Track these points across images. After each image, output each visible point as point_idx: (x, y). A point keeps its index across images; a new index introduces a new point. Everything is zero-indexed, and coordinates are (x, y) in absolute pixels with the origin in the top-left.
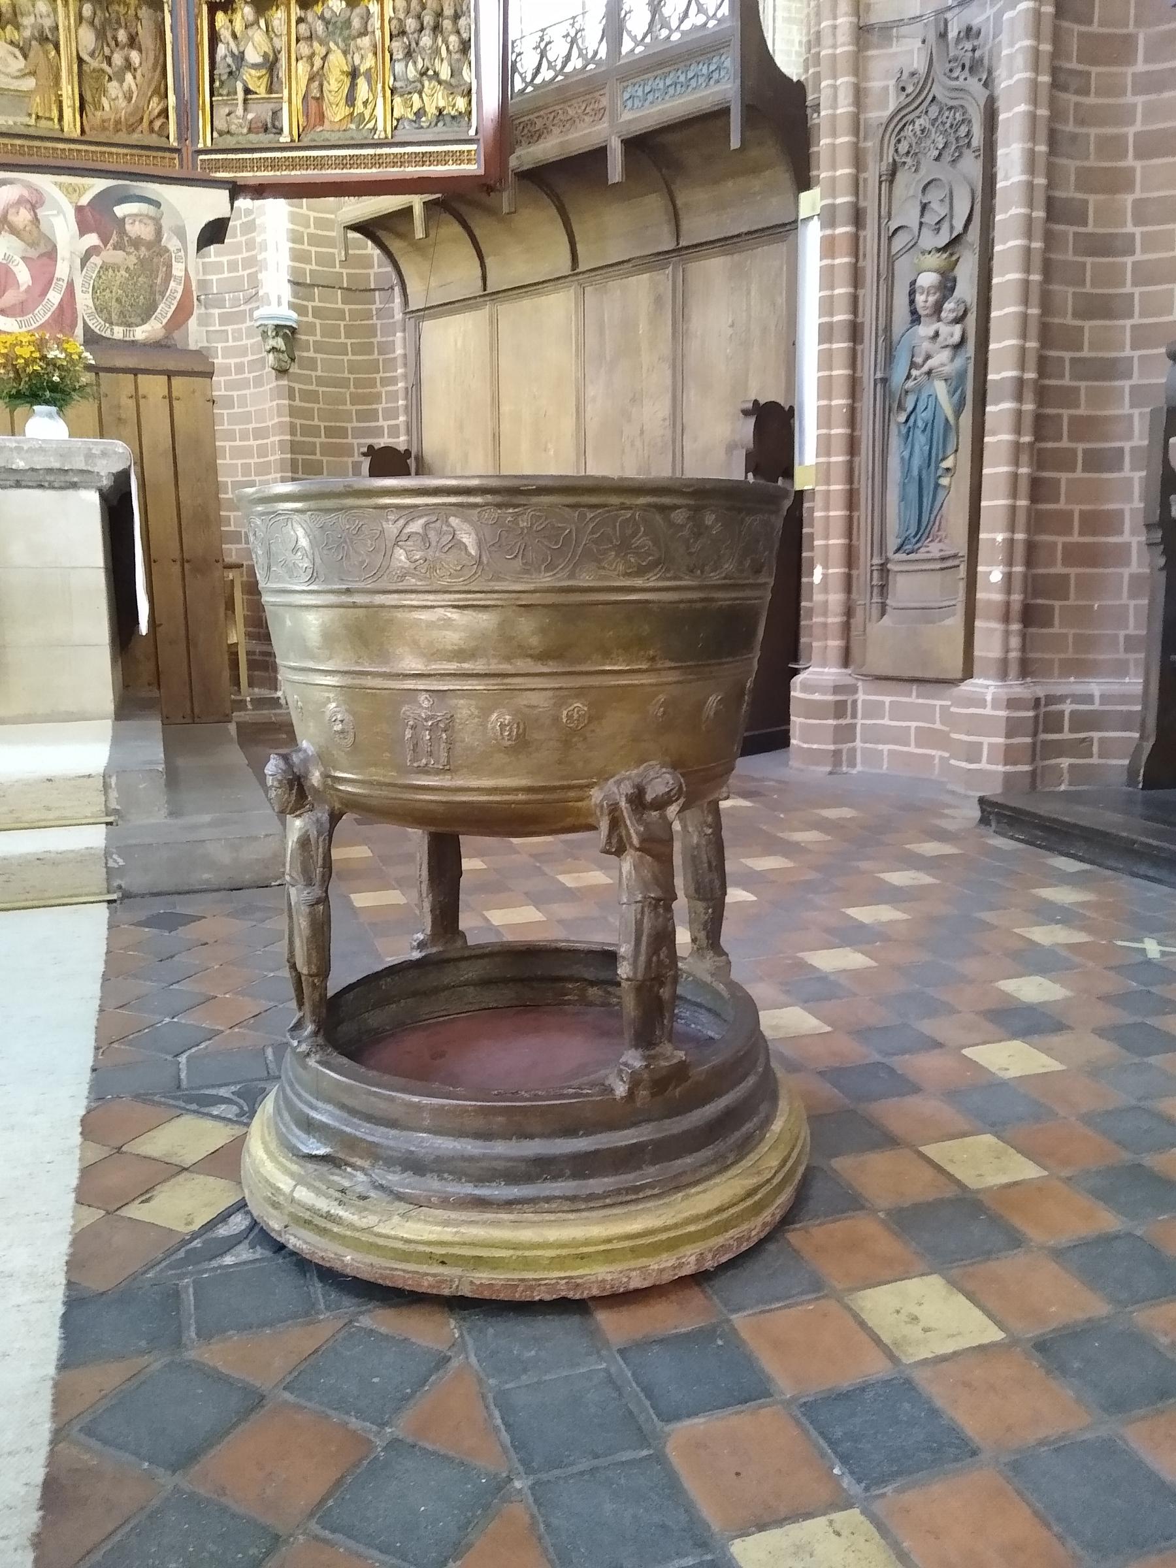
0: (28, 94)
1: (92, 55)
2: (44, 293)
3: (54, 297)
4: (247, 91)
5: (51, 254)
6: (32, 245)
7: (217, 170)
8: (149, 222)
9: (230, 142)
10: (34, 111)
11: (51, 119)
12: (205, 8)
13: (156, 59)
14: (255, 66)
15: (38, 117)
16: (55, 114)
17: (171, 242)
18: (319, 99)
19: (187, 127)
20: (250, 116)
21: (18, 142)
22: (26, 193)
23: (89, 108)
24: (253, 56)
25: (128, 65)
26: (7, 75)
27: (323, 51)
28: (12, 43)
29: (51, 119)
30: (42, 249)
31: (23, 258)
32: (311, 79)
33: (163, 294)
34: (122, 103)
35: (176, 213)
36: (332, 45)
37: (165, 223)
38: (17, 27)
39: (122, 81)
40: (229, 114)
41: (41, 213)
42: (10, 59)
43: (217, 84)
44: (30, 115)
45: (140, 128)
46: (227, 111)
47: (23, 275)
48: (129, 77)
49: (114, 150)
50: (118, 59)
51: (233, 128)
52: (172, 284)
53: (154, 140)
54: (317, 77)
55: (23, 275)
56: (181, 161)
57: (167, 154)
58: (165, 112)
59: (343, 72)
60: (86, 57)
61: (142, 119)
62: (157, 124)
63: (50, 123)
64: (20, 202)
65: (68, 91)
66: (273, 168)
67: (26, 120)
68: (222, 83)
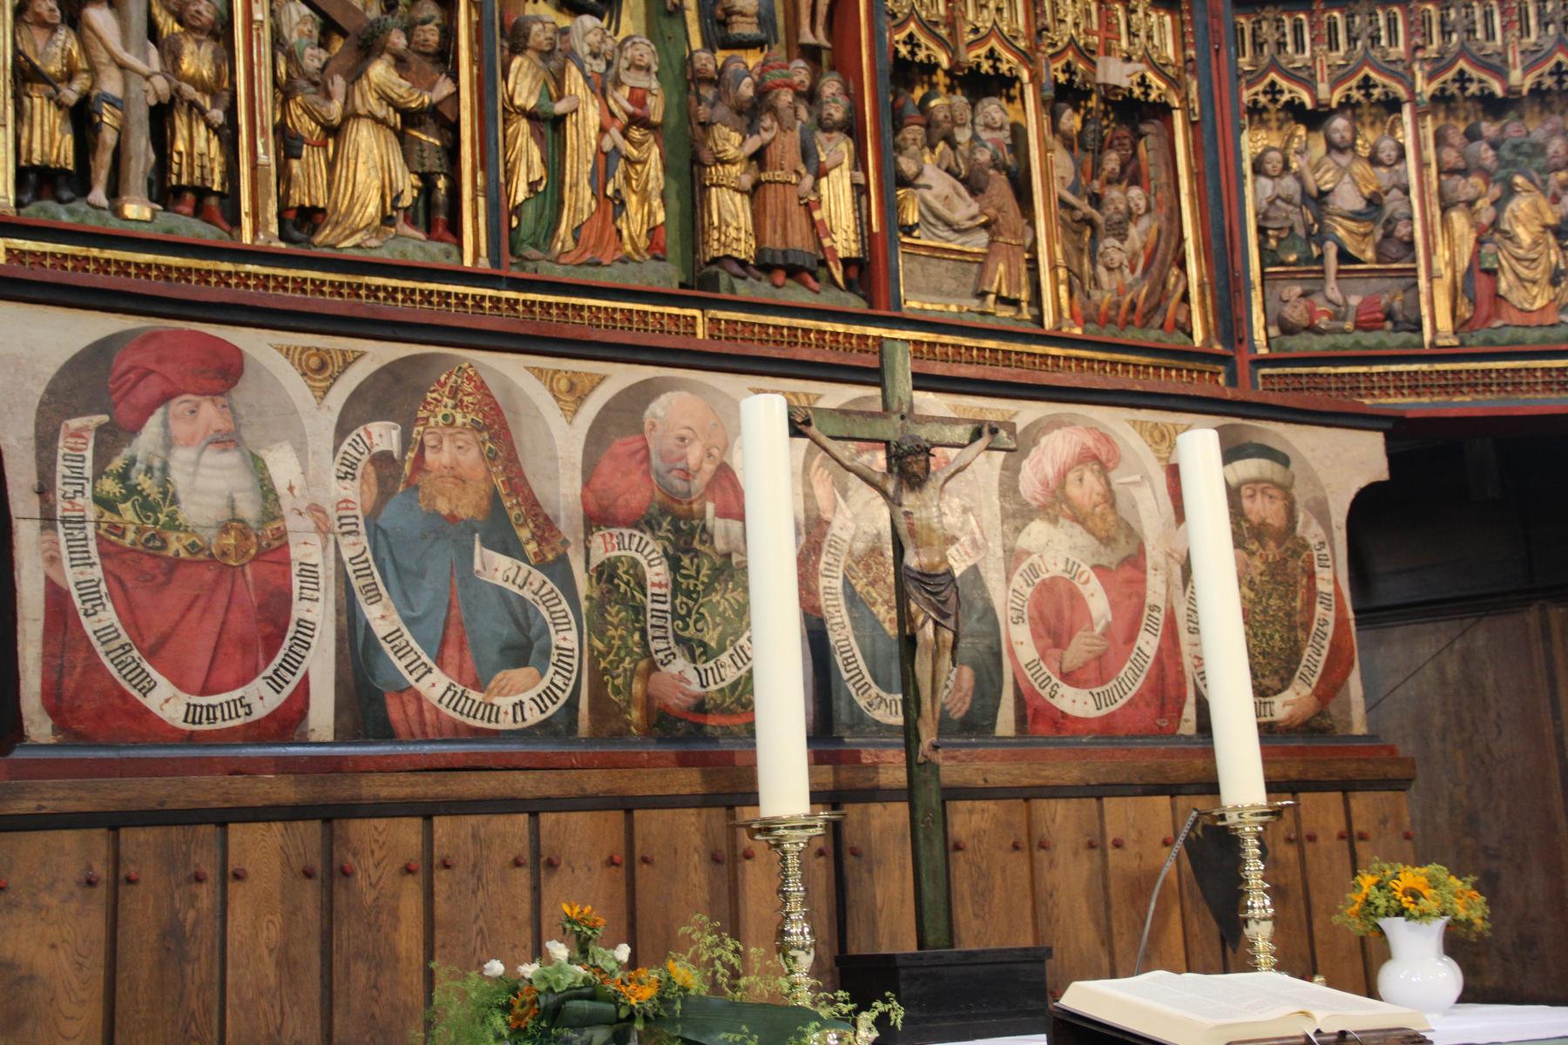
0: (982, 262)
2: (1131, 638)
3: (1148, 643)
4: (1344, 256)
5: (1136, 561)
6: (1107, 541)
8: (1274, 492)
9: (1317, 345)
10: (994, 289)
11: (1015, 303)
14: (1355, 216)
16: (1024, 295)
17: (1310, 531)
18: (1492, 273)
19: (1230, 322)
20: (1354, 301)
22: (1090, 443)
24: (1348, 198)
26: (949, 225)
27: (1495, 191)
30: (1124, 549)
31: (1095, 568)
32: (1480, 242)
33: (1307, 627)
35: (1312, 479)
36: (1519, 180)
37: (1300, 493)
39: (1123, 237)
40: (1304, 295)
41: (1117, 478)
43: (1273, 242)
44: (982, 295)
45: (1157, 320)
46: (1298, 290)
47: (1098, 604)
48: (1133, 231)
49: (1133, 358)
51: (1323, 322)
52: (1319, 609)
54: (1491, 232)
55: (1098, 604)
57: (1209, 367)
59: (1546, 227)
64: (1087, 457)
66: (1414, 390)
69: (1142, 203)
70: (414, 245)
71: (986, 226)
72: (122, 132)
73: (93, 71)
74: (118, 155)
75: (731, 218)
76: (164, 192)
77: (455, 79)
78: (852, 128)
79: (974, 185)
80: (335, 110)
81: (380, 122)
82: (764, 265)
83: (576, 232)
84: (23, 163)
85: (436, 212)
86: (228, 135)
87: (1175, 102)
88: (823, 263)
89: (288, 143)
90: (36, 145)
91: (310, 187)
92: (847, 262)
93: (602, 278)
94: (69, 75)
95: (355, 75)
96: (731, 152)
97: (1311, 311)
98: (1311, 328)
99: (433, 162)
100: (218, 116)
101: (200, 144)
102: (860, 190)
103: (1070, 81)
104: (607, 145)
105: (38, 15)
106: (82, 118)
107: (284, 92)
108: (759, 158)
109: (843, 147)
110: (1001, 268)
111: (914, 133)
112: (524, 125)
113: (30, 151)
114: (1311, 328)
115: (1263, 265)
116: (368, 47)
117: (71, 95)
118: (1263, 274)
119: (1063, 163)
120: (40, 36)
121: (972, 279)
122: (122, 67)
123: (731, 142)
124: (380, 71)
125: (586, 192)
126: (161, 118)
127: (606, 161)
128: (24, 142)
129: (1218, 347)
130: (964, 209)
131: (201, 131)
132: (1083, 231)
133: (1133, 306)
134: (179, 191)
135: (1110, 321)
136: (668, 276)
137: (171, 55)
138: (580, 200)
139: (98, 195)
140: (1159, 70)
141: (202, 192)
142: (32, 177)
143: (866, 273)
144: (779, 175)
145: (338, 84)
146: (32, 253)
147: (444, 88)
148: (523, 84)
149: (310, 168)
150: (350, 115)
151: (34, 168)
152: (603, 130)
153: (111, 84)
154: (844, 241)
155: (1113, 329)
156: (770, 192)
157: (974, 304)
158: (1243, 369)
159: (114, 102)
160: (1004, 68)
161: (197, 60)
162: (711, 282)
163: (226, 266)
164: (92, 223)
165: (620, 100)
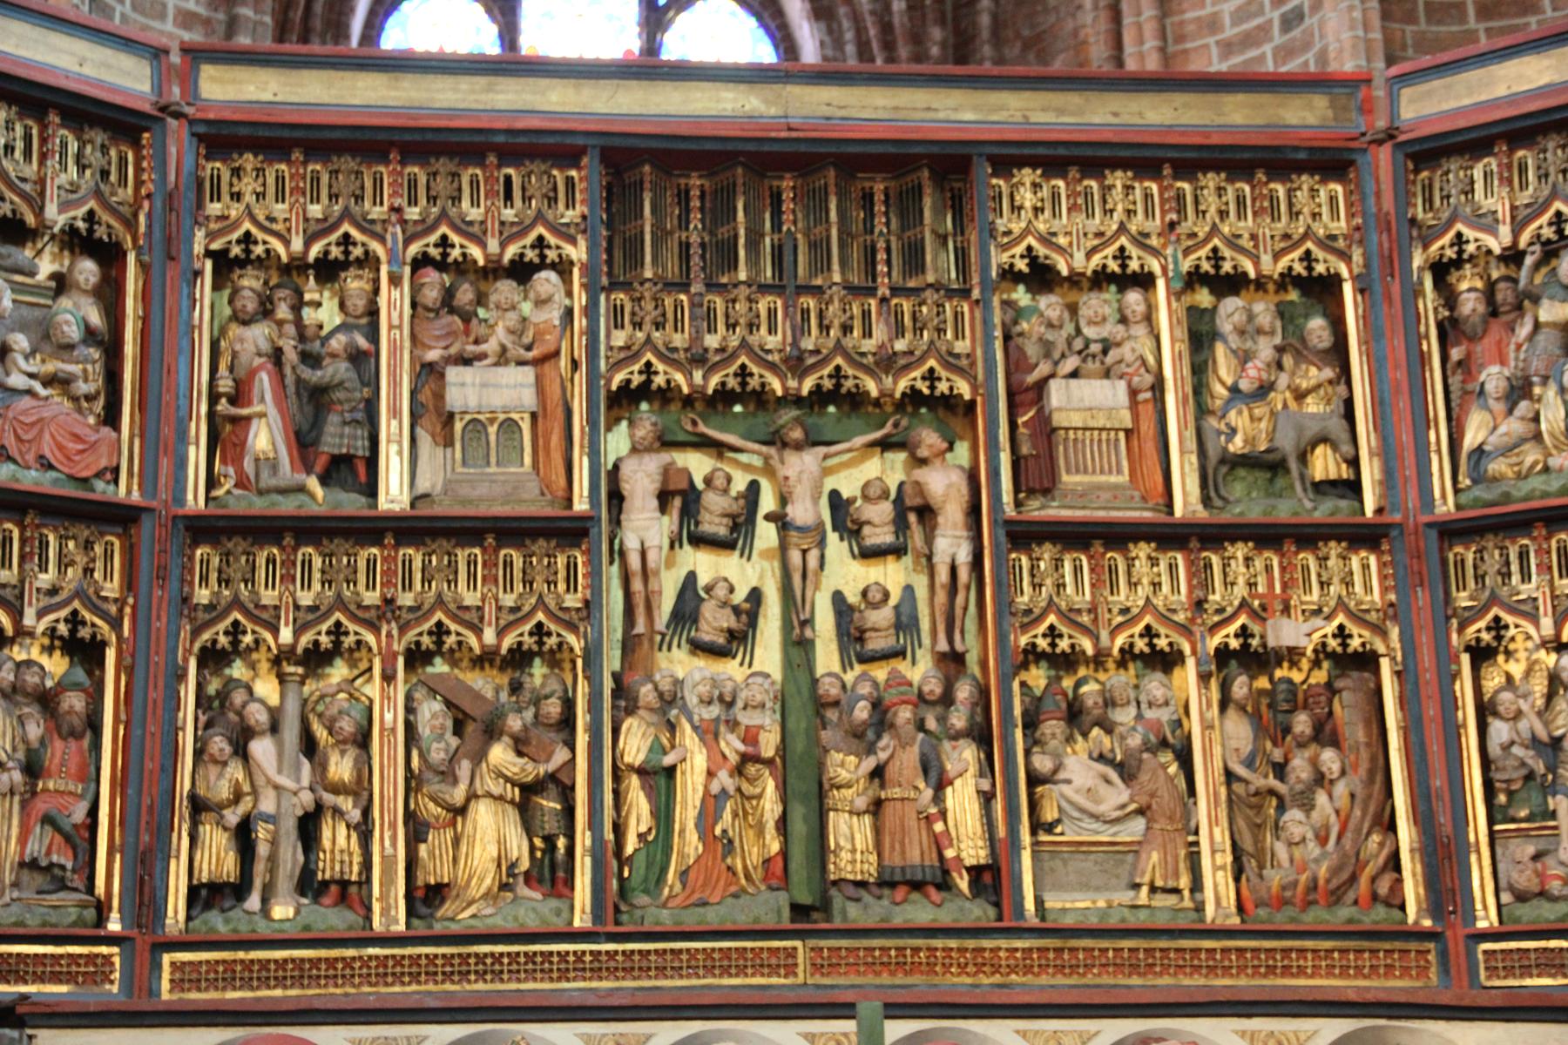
0: (1135, 849)
1: (1249, 763)
7: (1526, 971)
9: (1547, 913)
10: (1146, 879)
11: (1176, 891)
12: (1465, 659)
13: (1373, 759)
15: (1153, 889)
16: (1184, 882)
21: (1126, 944)
23: (1251, 865)
25: (1320, 779)
26: (1096, 817)
28: (1101, 758)
29: (1176, 891)
34: (1313, 849)
38: (1109, 729)
40: (1536, 857)
42: (1103, 789)
43: (1502, 798)
45: (1351, 896)
46: (1531, 849)
48: (1321, 798)
50: (1300, 766)
53: (1379, 916)
56: (1444, 956)
57: (1413, 945)
58: (1394, 862)
60: (1241, 770)
61: (1353, 878)
62: (1383, 888)
63: (1171, 900)
65: (1213, 837)
67: (1127, 897)
68: (1511, 794)
69: (1336, 767)
70: (532, 909)
71: (1141, 812)
72: (274, 843)
73: (255, 792)
74: (272, 859)
75: (852, 842)
76: (309, 884)
77: (572, 749)
78: (981, 736)
79: (1127, 771)
80: (458, 794)
81: (500, 798)
82: (887, 882)
83: (684, 875)
84: (195, 882)
85: (551, 872)
86: (364, 831)
87: (1381, 648)
88: (946, 872)
89: (416, 830)
90: (205, 866)
91: (435, 870)
92: (976, 872)
93: (712, 917)
94: (237, 797)
95: (479, 756)
96: (844, 775)
97: (1541, 876)
98: (1543, 894)
99: (551, 825)
100: (355, 815)
101: (341, 841)
102: (987, 798)
103: (1245, 646)
104: (715, 788)
105: (212, 755)
106: (243, 835)
107: (413, 783)
108: (878, 773)
109: (968, 753)
110: (1155, 857)
111: (1052, 728)
112: (635, 781)
113: (201, 871)
114: (1543, 894)
115: (1491, 822)
116: (492, 732)
117: (232, 817)
118: (1492, 835)
119: (1239, 731)
120: (213, 771)
121: (1124, 871)
122: (277, 787)
123: (846, 767)
124: (500, 754)
125: (692, 837)
126: (309, 827)
127: (712, 805)
128: (196, 864)
129: (1427, 923)
130: (1116, 796)
131: (342, 831)
132: (1253, 809)
133: (1313, 886)
134: (325, 884)
135: (1282, 902)
136: (770, 907)
137: (320, 767)
138: (689, 843)
139: (254, 902)
140: (1358, 618)
141: (344, 884)
142: (204, 892)
143: (991, 879)
144: (895, 792)
145: (464, 768)
146: (191, 963)
147: (561, 755)
148: (636, 743)
149: (435, 846)
150: (472, 796)
151: (203, 885)
152: (710, 774)
153: (267, 805)
154: (971, 849)
155: (1289, 911)
156: (889, 810)
157: (1127, 897)
158: (1456, 946)
159: (268, 819)
160: (1162, 643)
161: (341, 767)
162: (825, 906)
163: (350, 952)
164: (244, 929)
165: (732, 745)
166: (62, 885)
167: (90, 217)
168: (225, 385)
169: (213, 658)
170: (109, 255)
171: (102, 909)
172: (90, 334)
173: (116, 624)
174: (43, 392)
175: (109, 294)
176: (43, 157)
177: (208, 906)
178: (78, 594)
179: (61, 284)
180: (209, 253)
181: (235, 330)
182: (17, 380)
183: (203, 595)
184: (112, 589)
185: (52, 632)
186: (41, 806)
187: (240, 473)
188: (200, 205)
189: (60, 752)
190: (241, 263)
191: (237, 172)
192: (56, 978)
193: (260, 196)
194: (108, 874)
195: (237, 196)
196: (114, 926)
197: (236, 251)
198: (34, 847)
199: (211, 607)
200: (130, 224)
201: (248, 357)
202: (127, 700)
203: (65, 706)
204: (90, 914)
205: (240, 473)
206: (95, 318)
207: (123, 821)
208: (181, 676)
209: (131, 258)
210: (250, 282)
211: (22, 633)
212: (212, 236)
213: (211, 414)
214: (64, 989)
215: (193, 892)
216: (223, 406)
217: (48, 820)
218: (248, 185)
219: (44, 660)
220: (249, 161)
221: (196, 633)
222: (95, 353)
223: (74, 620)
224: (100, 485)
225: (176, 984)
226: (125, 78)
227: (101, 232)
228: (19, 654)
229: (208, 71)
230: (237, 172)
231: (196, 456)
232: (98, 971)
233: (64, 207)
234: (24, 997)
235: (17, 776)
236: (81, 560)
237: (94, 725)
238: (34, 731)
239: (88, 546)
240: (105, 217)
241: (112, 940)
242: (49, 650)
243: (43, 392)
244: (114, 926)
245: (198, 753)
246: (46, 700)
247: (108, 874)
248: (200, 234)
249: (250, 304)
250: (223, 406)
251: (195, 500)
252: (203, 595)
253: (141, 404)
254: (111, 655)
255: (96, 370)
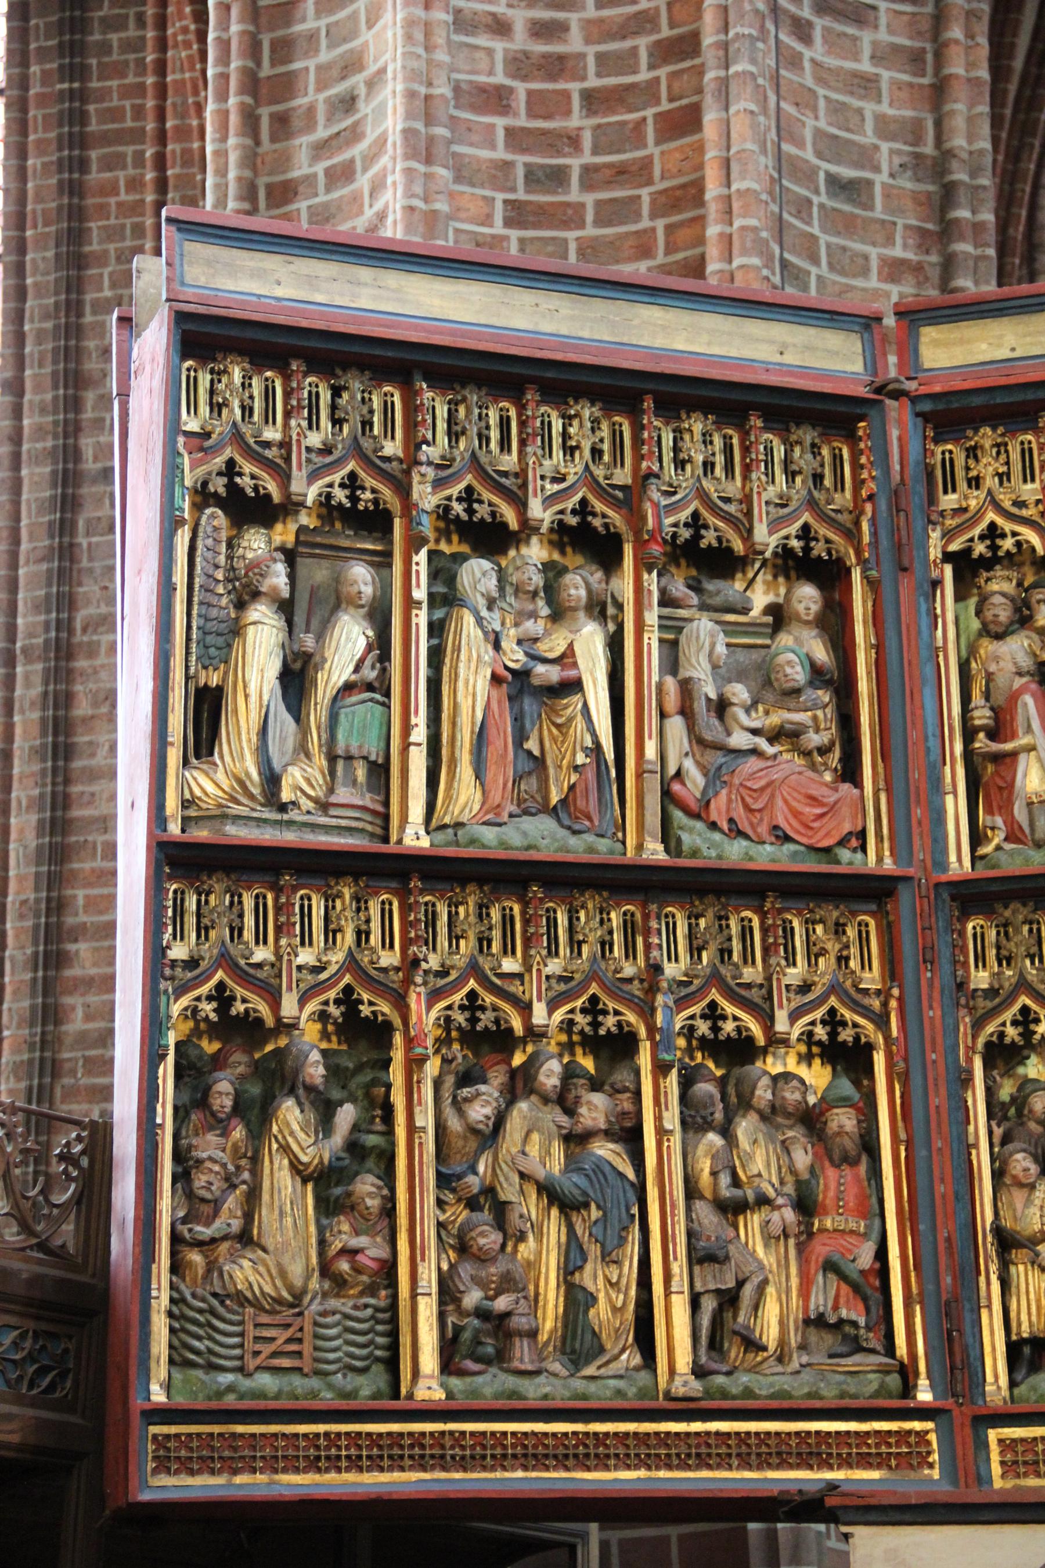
84: (1014, 1338)
90: (1024, 1317)
105: (1014, 1177)
113: (1019, 1325)
120: (1019, 1196)
128: (1013, 1315)
142: (1027, 1350)
146: (1023, 1440)
151: (1023, 1341)
166: (857, 1347)
167: (805, 535)
168: (982, 716)
169: (1002, 1056)
170: (830, 575)
171: (907, 1374)
172: (817, 674)
173: (881, 1021)
174: (770, 750)
175: (835, 623)
176: (747, 469)
177: (1034, 1368)
178: (834, 989)
179: (779, 617)
180: (948, 557)
181: (987, 647)
182: (740, 739)
183: (981, 979)
184: (872, 978)
185: (808, 1037)
186: (820, 1249)
187: (1011, 824)
188: (932, 499)
189: (835, 1184)
190: (988, 563)
191: (973, 452)
192: (865, 1461)
193: (1003, 477)
194: (909, 1331)
195: (975, 482)
196: (924, 1395)
197: (980, 549)
198: (819, 1300)
199: (992, 992)
200: (852, 534)
201: (1006, 679)
202: (904, 1114)
203: (833, 1126)
204: (894, 1381)
205: (1011, 824)
206: (821, 653)
207: (917, 1263)
208: (966, 1081)
209: (856, 575)
210: (1000, 585)
211: (776, 1041)
212: (949, 535)
213: (968, 755)
214: (875, 1475)
215: (1014, 1350)
216: (981, 742)
217: (830, 1266)
218: (988, 467)
219: (803, 1071)
220: (986, 436)
221: (978, 1025)
222: (824, 696)
223: (833, 1020)
224: (845, 855)
225: (1009, 1468)
226: (832, 359)
227: (819, 550)
228: (773, 1066)
229: (929, 334)
230: (973, 452)
231: (955, 806)
232: (913, 1452)
233: (774, 526)
234: (832, 1487)
235: (789, 1215)
236: (833, 947)
237: (870, 1146)
238: (802, 1159)
239: (839, 929)
240: (822, 530)
241: (923, 1413)
242: (807, 1058)
243: (770, 750)
244: (924, 1395)
245: (998, 1175)
246: (811, 1120)
247: (909, 1331)
248: (935, 535)
249: (1002, 612)
250: (981, 742)
251: (959, 862)
252: (981, 979)
253: (884, 752)
254: (879, 1060)
255: (827, 716)
